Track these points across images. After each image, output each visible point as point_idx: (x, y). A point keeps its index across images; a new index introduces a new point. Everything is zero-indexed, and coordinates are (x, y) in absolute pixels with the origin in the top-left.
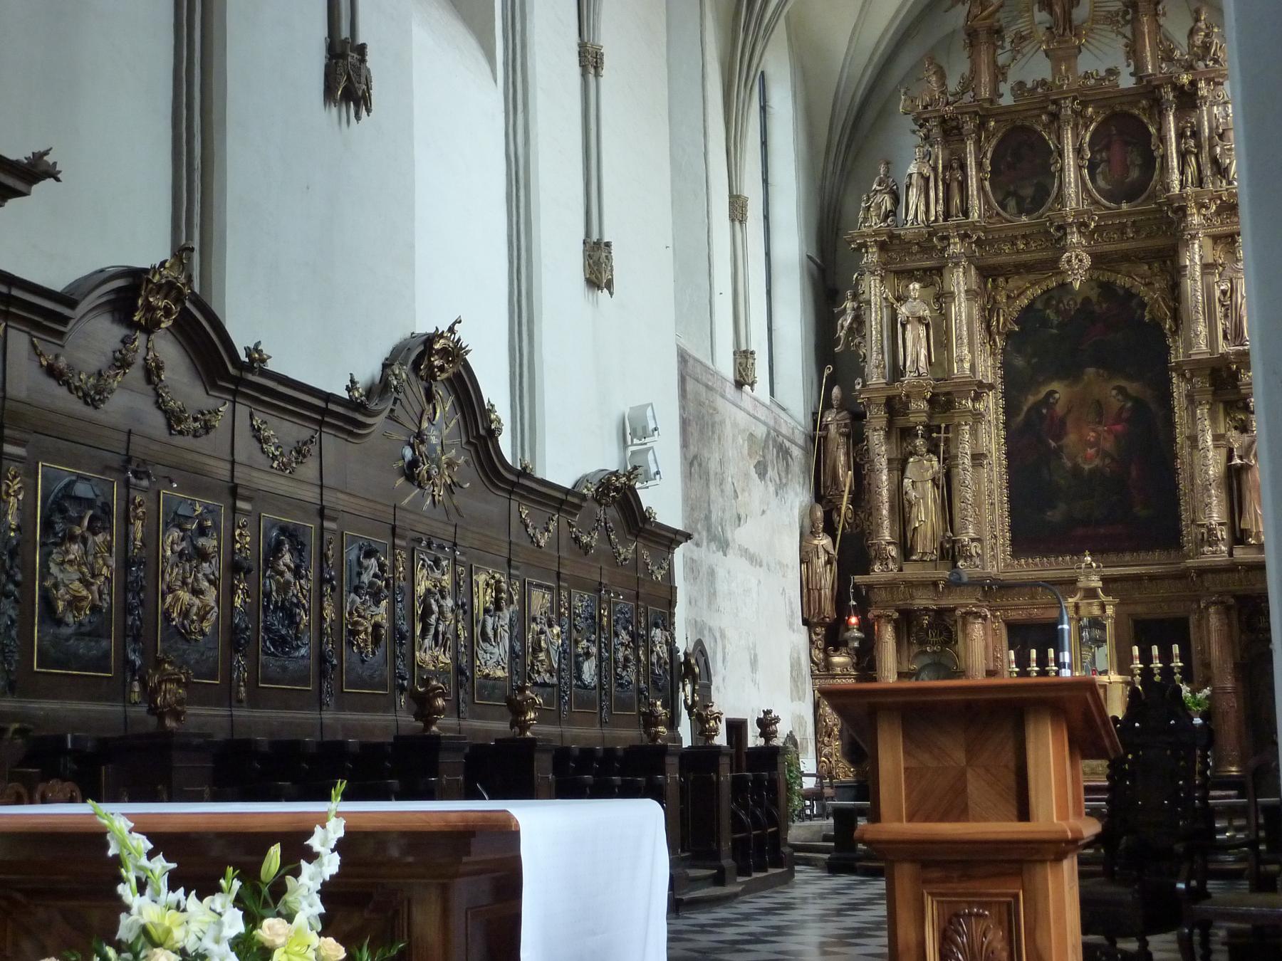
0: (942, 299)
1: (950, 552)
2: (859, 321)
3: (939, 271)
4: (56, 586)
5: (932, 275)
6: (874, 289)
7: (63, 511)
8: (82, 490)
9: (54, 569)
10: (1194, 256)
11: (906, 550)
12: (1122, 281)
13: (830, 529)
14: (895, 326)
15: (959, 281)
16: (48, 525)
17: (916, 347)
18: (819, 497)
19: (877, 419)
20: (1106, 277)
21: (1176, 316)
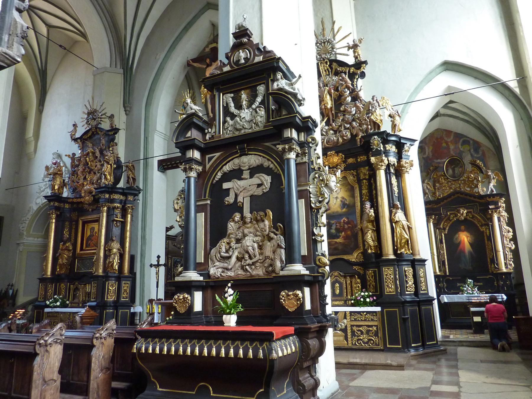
4: (175, 273)
7: (176, 263)
8: (178, 260)
9: (175, 271)
16: (174, 265)
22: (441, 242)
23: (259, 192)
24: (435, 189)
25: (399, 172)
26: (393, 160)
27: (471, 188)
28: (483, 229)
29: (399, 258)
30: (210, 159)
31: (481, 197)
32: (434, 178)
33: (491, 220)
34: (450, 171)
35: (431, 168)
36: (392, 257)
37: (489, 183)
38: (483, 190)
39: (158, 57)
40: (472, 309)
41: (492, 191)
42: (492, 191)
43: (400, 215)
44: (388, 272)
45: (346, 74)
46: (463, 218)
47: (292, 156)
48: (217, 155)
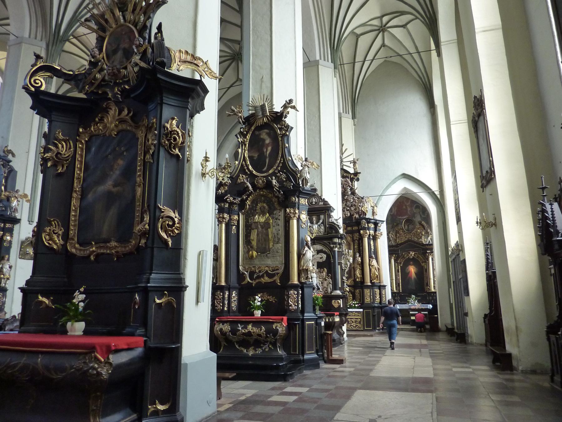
22: (398, 272)
23: (321, 261)
24: (396, 237)
25: (375, 238)
26: (372, 232)
27: (418, 238)
28: (423, 264)
29: (373, 285)
31: (423, 245)
32: (396, 231)
33: (428, 259)
34: (406, 227)
35: (395, 224)
36: (370, 284)
37: (428, 237)
38: (425, 241)
40: (411, 313)
41: (429, 242)
42: (429, 242)
43: (374, 262)
44: (367, 292)
45: (348, 178)
46: (412, 258)
47: (336, 249)
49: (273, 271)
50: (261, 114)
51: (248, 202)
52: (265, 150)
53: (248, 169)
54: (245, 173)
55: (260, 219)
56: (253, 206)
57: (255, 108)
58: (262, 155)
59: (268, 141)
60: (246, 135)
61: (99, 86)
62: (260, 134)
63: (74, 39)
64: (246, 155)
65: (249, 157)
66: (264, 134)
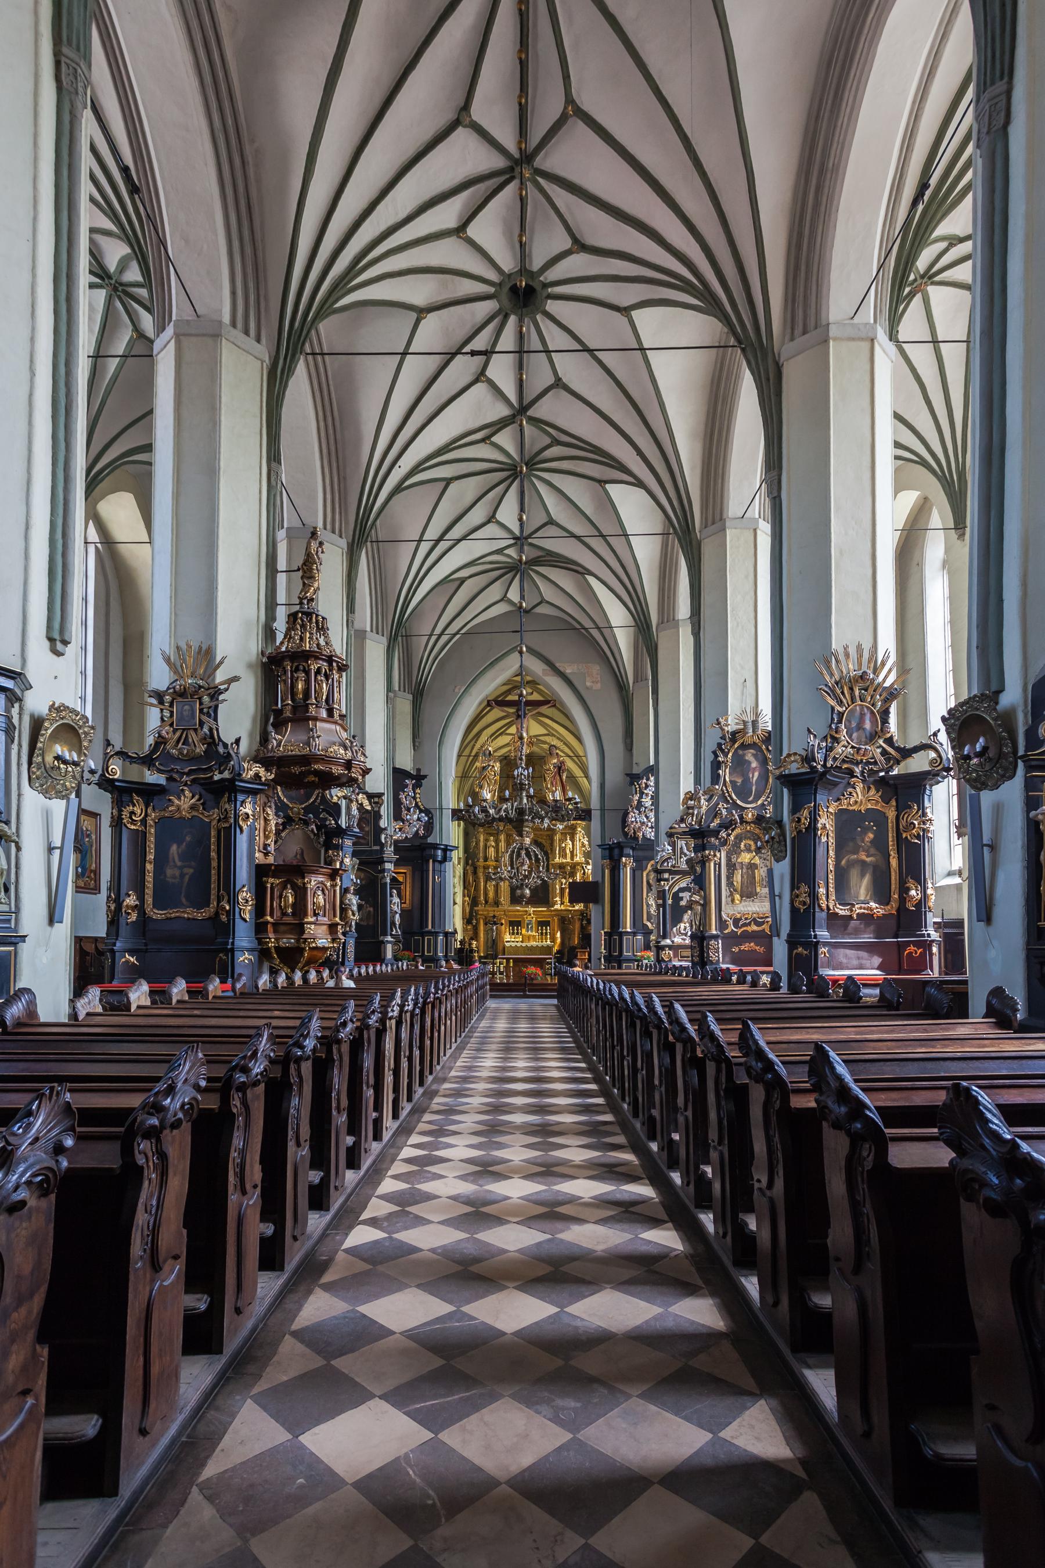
0: (497, 841)
1: (497, 903)
2: (477, 843)
3: (497, 834)
5: (496, 835)
6: (482, 838)
10: (557, 837)
11: (486, 902)
12: (540, 840)
13: (469, 896)
14: (486, 847)
15: (502, 837)
17: (492, 852)
18: (465, 888)
19: (481, 870)
20: (536, 839)
21: (551, 850)
30: (672, 879)
39: (457, 690)
48: (678, 877)
49: (762, 918)
50: (751, 731)
51: (732, 838)
52: (751, 776)
53: (730, 796)
54: (727, 802)
55: (746, 857)
56: (736, 843)
57: (745, 723)
58: (746, 781)
59: (754, 764)
60: (728, 753)
61: (844, 761)
62: (744, 755)
63: (587, 626)
64: (727, 779)
65: (730, 781)
66: (750, 755)
